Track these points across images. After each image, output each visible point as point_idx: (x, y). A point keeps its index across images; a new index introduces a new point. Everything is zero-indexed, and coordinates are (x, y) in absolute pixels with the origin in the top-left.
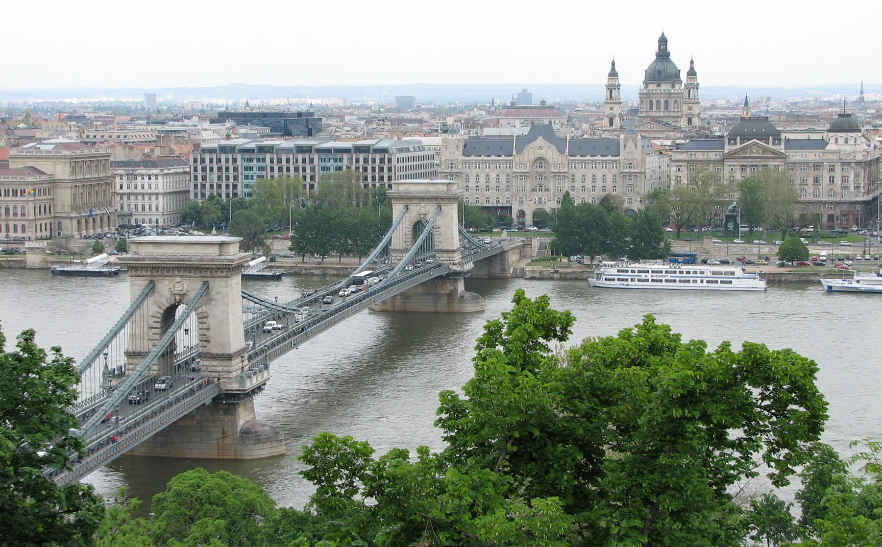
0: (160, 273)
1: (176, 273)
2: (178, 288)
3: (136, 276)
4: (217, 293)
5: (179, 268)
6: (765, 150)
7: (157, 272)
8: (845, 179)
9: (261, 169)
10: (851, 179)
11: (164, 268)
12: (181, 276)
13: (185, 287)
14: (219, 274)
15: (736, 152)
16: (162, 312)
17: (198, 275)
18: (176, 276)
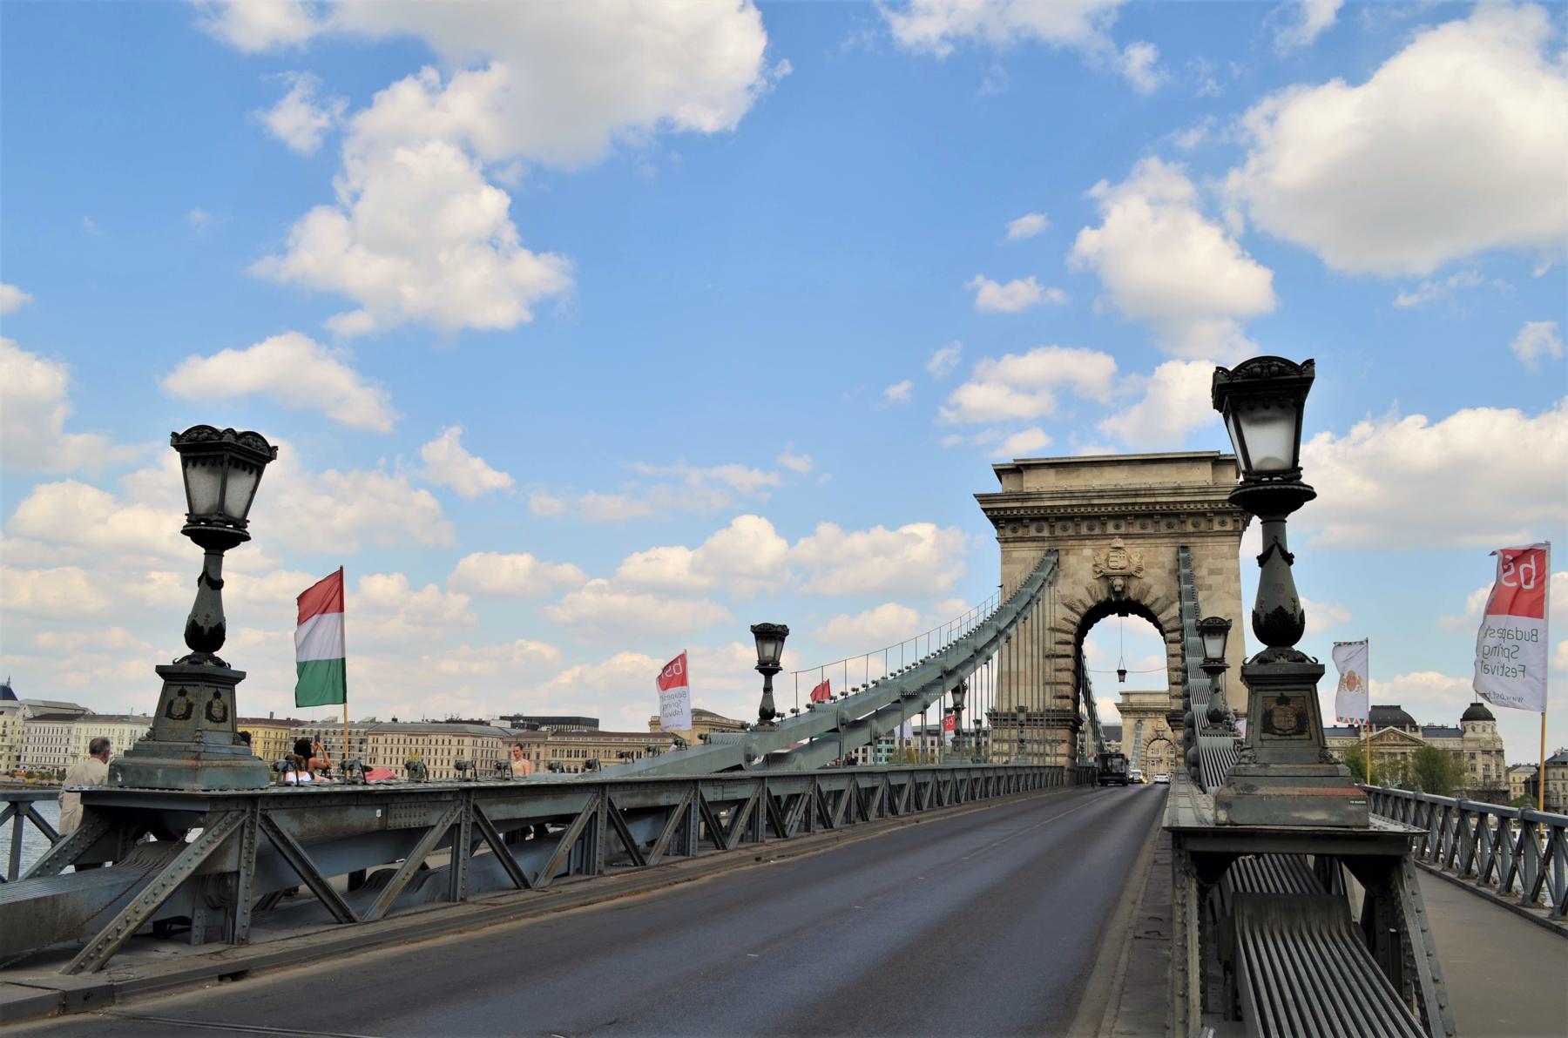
0: (1071, 532)
1: (1111, 529)
2: (1118, 561)
3: (1016, 540)
4: (1212, 572)
5: (1119, 517)
6: (1403, 737)
7: (1065, 529)
8: (1487, 767)
9: (889, 751)
10: (1493, 767)
11: (1084, 518)
12: (1125, 536)
13: (1135, 560)
14: (1217, 527)
15: (1372, 739)
16: (1077, 618)
17: (1163, 529)
18: (1112, 536)
